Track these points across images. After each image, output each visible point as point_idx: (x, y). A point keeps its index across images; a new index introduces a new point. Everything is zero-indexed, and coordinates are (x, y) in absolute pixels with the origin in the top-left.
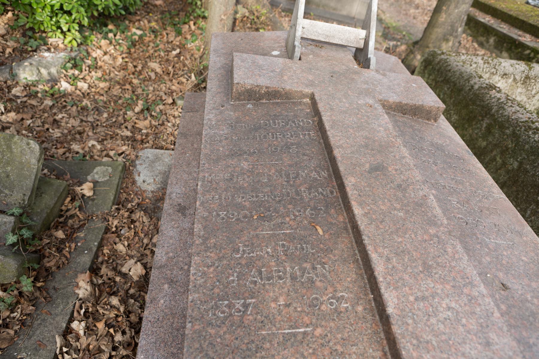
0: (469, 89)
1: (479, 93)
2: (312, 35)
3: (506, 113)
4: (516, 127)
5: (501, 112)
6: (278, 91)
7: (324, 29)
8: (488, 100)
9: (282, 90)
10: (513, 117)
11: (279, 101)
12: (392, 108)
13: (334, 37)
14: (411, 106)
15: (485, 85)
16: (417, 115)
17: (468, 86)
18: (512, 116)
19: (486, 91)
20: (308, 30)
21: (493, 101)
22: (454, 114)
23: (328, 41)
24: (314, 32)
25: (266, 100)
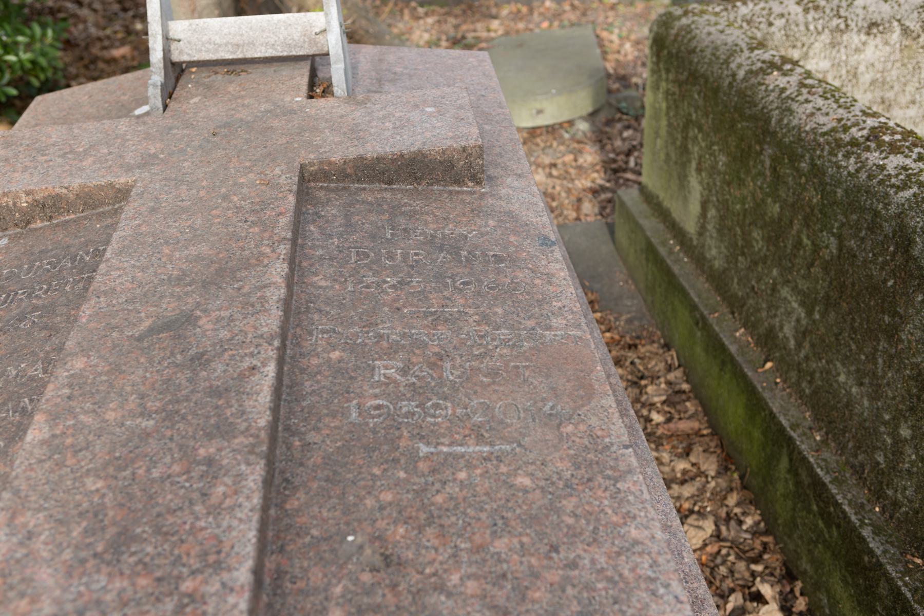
0: (730, 83)
1: (746, 88)
2: (201, 51)
3: (795, 122)
4: (814, 150)
5: (785, 121)
6: (58, 195)
7: (226, 31)
8: (762, 98)
9: (64, 191)
10: (807, 128)
11: (72, 216)
12: (348, 176)
13: (253, 44)
14: (393, 161)
15: (759, 65)
16: (421, 178)
17: (727, 76)
18: (806, 125)
19: (759, 78)
20: (189, 43)
21: (771, 98)
22: (720, 150)
23: (241, 56)
24: (203, 45)
25: (42, 221)
